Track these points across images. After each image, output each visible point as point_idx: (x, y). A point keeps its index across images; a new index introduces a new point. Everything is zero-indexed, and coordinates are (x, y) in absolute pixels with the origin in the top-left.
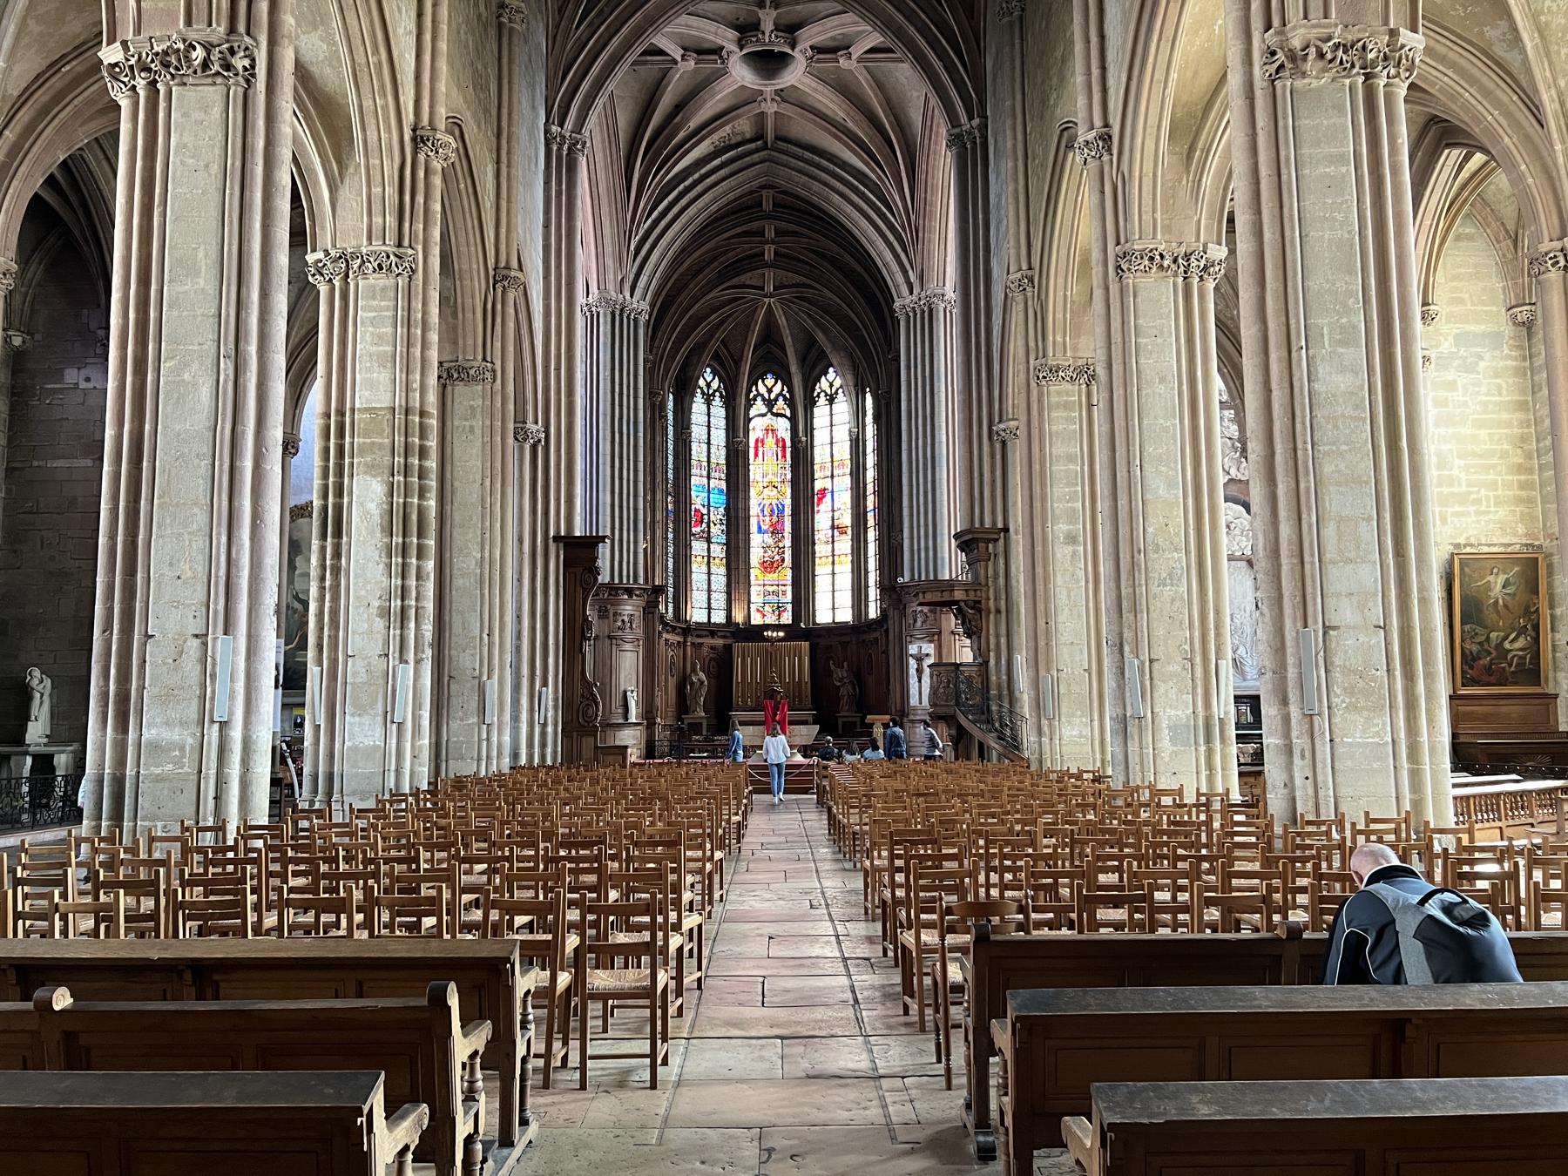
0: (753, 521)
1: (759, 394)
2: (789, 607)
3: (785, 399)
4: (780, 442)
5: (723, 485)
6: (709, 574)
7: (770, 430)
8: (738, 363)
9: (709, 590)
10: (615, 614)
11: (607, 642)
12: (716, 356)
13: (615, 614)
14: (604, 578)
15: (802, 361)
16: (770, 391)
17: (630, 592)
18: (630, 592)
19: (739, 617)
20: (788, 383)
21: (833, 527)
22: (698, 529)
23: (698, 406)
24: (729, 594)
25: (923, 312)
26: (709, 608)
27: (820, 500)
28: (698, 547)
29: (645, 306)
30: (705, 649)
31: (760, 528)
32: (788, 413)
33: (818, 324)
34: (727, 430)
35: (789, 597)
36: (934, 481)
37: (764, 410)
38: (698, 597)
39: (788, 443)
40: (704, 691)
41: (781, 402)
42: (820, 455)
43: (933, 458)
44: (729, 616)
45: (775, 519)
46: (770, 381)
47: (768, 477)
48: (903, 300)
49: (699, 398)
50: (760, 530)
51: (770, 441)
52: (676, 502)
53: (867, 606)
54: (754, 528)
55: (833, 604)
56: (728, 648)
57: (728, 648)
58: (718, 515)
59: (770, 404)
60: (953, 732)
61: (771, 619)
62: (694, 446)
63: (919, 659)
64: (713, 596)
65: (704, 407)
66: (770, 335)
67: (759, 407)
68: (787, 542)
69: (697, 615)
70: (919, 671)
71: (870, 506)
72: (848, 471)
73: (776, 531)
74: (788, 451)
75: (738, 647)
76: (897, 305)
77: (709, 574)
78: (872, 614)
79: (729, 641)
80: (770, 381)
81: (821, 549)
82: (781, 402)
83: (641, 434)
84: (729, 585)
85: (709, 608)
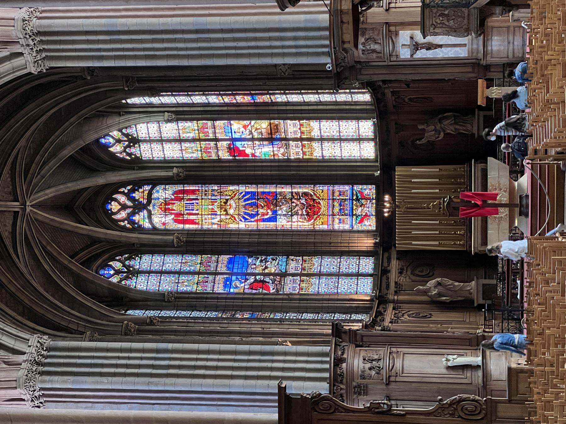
0: (263, 225)
2: (357, 188)
3: (133, 191)
4: (178, 196)
6: (320, 275)
7: (166, 208)
8: (94, 241)
9: (338, 275)
10: (363, 377)
11: (393, 386)
12: (87, 263)
13: (363, 377)
14: (323, 388)
15: (92, 171)
17: (339, 361)
18: (339, 361)
19: (368, 243)
20: (115, 188)
21: (271, 140)
23: (141, 284)
24: (341, 254)
25: (41, 42)
26: (358, 275)
28: (290, 286)
29: (34, 339)
30: (402, 280)
31: (269, 220)
32: (147, 188)
33: (54, 155)
34: (165, 253)
36: (222, 31)
38: (345, 287)
39: (180, 187)
41: (136, 195)
42: (192, 153)
43: (197, 31)
44: (366, 254)
46: (114, 207)
47: (217, 211)
48: (29, 63)
50: (273, 219)
51: (177, 207)
52: (242, 309)
53: (356, 103)
54: (271, 225)
55: (354, 141)
56: (403, 255)
57: (403, 255)
59: (138, 207)
60: (498, 10)
61: (370, 208)
62: (182, 288)
63: (416, 47)
64: (344, 270)
65: (142, 278)
66: (66, 205)
67: (141, 218)
68: (287, 190)
70: (430, 47)
72: (209, 123)
73: (273, 201)
74: (187, 188)
75: (400, 244)
76: (34, 70)
77: (320, 275)
78: (366, 97)
79: (394, 255)
80: (114, 207)
81: (295, 152)
82: (136, 195)
83: (170, 346)
84: (332, 254)
85: (358, 275)
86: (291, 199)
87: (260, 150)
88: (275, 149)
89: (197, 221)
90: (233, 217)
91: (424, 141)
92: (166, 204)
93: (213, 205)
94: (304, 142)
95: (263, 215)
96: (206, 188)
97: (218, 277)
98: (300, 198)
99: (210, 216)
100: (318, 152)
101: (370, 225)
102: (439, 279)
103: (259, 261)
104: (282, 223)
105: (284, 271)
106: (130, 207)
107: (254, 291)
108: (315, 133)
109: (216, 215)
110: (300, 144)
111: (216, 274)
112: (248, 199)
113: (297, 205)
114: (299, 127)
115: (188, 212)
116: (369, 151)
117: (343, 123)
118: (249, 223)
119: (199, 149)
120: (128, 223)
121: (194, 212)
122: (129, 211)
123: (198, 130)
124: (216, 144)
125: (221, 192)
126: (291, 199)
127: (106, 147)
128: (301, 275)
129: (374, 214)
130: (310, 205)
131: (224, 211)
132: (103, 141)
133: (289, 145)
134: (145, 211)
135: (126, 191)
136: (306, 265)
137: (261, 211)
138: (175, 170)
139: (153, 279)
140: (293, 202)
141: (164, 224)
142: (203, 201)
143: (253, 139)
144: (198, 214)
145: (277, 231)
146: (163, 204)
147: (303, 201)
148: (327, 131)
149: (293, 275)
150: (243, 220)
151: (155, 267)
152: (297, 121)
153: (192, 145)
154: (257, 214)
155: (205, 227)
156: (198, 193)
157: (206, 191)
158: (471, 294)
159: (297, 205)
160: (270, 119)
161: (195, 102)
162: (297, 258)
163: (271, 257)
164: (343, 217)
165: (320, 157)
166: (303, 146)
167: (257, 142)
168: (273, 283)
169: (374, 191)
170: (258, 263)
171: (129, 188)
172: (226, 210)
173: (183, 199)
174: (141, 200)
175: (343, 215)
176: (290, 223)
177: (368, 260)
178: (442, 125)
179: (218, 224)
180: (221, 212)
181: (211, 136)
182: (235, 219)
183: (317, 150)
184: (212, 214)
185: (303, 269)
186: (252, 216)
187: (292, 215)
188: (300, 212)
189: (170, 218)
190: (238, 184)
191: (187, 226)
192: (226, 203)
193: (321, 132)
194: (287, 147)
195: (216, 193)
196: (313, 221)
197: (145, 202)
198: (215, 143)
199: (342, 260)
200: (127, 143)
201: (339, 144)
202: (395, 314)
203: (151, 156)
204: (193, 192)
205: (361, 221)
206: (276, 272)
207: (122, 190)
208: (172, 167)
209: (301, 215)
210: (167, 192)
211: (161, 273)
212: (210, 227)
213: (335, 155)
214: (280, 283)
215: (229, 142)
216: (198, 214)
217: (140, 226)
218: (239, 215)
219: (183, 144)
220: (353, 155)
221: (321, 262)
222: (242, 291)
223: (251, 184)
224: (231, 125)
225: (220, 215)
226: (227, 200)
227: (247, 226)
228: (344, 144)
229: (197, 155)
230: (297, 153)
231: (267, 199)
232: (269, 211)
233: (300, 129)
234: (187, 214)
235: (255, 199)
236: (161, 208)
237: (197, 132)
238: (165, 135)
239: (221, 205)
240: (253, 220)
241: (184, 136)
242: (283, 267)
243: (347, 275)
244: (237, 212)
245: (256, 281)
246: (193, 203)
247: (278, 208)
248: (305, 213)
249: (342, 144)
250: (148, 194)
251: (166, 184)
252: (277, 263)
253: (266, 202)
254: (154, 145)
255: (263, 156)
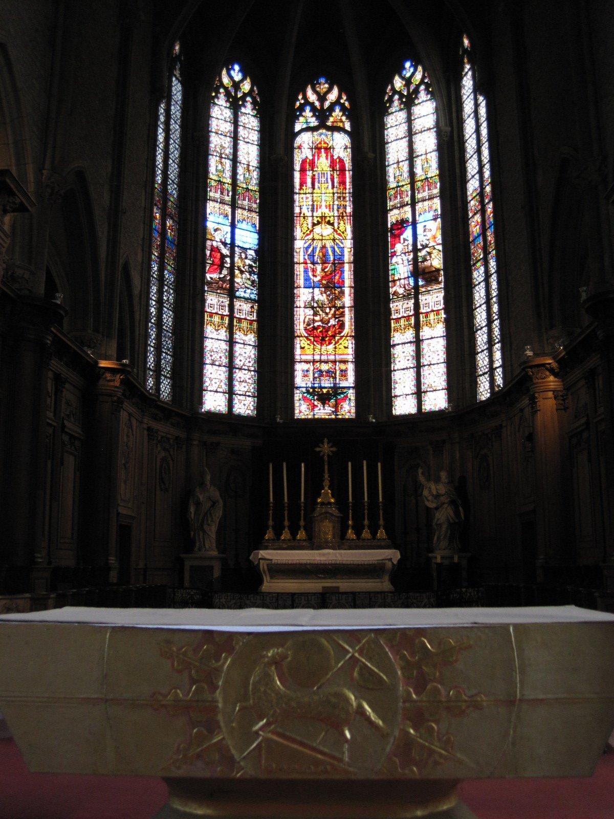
0: (299, 270)
1: (307, 102)
2: (351, 394)
3: (343, 108)
4: (337, 165)
5: (256, 218)
6: (231, 342)
9: (231, 367)
16: (322, 98)
22: (215, 276)
23: (220, 114)
27: (397, 237)
28: (214, 302)
31: (307, 279)
32: (348, 126)
35: (350, 380)
37: (314, 122)
38: (214, 376)
39: (348, 165)
40: (218, 513)
41: (337, 112)
45: (329, 267)
49: (222, 101)
51: (323, 163)
54: (300, 281)
55: (420, 382)
58: (246, 260)
59: (322, 115)
61: (323, 412)
62: (213, 162)
64: (238, 375)
65: (228, 113)
67: (309, 118)
68: (348, 300)
69: (214, 402)
71: (475, 227)
72: (436, 191)
73: (331, 285)
74: (348, 175)
77: (231, 342)
78: (484, 391)
81: (400, 308)
82: (337, 112)
86: (334, 307)
87: (400, 262)
88: (402, 281)
89: (304, 188)
90: (310, 232)
91: (422, 479)
92: (327, 149)
93: (326, 206)
94: (413, 319)
95: (314, 271)
96: (347, 199)
97: (228, 209)
98: (336, 318)
99: (311, 203)
100: (401, 338)
101: (300, 412)
102: (221, 503)
103: (251, 263)
104: (303, 295)
105: (237, 294)
106: (322, 105)
107: (208, 253)
108: (425, 332)
109: (313, 211)
110: (411, 314)
111: (234, 206)
112: (334, 251)
113: (327, 314)
114: (435, 309)
115: (316, 177)
116: (404, 406)
117: (442, 368)
118: (302, 253)
119: (400, 184)
120: (300, 103)
121: (317, 185)
122: (317, 104)
123: (427, 178)
124: (407, 204)
125: (343, 217)
126: (334, 307)
127: (400, 70)
128: (231, 316)
129: (316, 417)
130: (327, 331)
131: (318, 221)
132: (408, 65)
133: (409, 299)
134: (316, 124)
135: (342, 101)
136: (244, 324)
137: (319, 268)
138: (371, 155)
139: (228, 127)
140: (330, 310)
141: (300, 147)
142: (332, 195)
143: (415, 250)
144: (313, 187)
145: (293, 288)
146: (325, 145)
147: (332, 322)
148: (431, 347)
149: (231, 307)
150: (306, 245)
151: (242, 132)
152: (442, 306)
153: (406, 175)
154: (313, 263)
155: (296, 197)
156: (342, 188)
157: (344, 198)
158: (200, 550)
159: (327, 314)
160: (445, 269)
161: (468, 165)
162: (255, 314)
163: (257, 280)
164: (312, 375)
165: (394, 341)
166: (408, 318)
167: (411, 256)
168: (219, 278)
169: (347, 417)
170: (248, 262)
171: (347, 104)
172: (319, 223)
173: (333, 170)
174: (331, 119)
175: (314, 374)
176: (302, 305)
177: (252, 408)
178: (445, 506)
179: (300, 213)
180: (317, 217)
181: (419, 196)
182: (308, 235)
183: (402, 337)
184: (313, 205)
185: (240, 320)
186: (312, 255)
187: (313, 308)
188: (317, 318)
189: (306, 153)
190: (354, 238)
191: (297, 175)
192: (329, 223)
193: (428, 339)
194: (406, 297)
195: (341, 211)
196: (306, 335)
197: (329, 124)
198: (409, 202)
199: (253, 373)
200: (405, 93)
201: (412, 366)
202: (168, 439)
203: (389, 126)
204: (342, 182)
205: (305, 399)
206: (236, 285)
207: (345, 98)
208: (374, 151)
209: (314, 320)
210: (343, 149)
211: (235, 138)
212: (297, 204)
213: (397, 362)
214: (219, 288)
215: (410, 220)
216: (313, 187)
217: (297, 118)
218: (313, 240)
219: (407, 162)
220: (396, 386)
221: (250, 345)
222: (209, 237)
223: (355, 255)
224: (435, 219)
225: (313, 216)
226: (332, 224)
227: (298, 250)
228: (412, 373)
229: (392, 184)
230: (397, 311)
231: (335, 276)
232: (319, 278)
233: (433, 311)
234: (314, 175)
235: (334, 260)
236: (320, 143)
237: (423, 177)
238: (417, 139)
239: (325, 217)
240: (306, 257)
241: (418, 163)
242: (242, 294)
243: (231, 379)
244: (317, 237)
245: (223, 257)
246: (327, 182)
247: (323, 289)
248: (316, 324)
249: (412, 370)
250: (339, 127)
251: (353, 148)
252: (248, 286)
253: (331, 274)
254: (404, 127)
255: (393, 267)
